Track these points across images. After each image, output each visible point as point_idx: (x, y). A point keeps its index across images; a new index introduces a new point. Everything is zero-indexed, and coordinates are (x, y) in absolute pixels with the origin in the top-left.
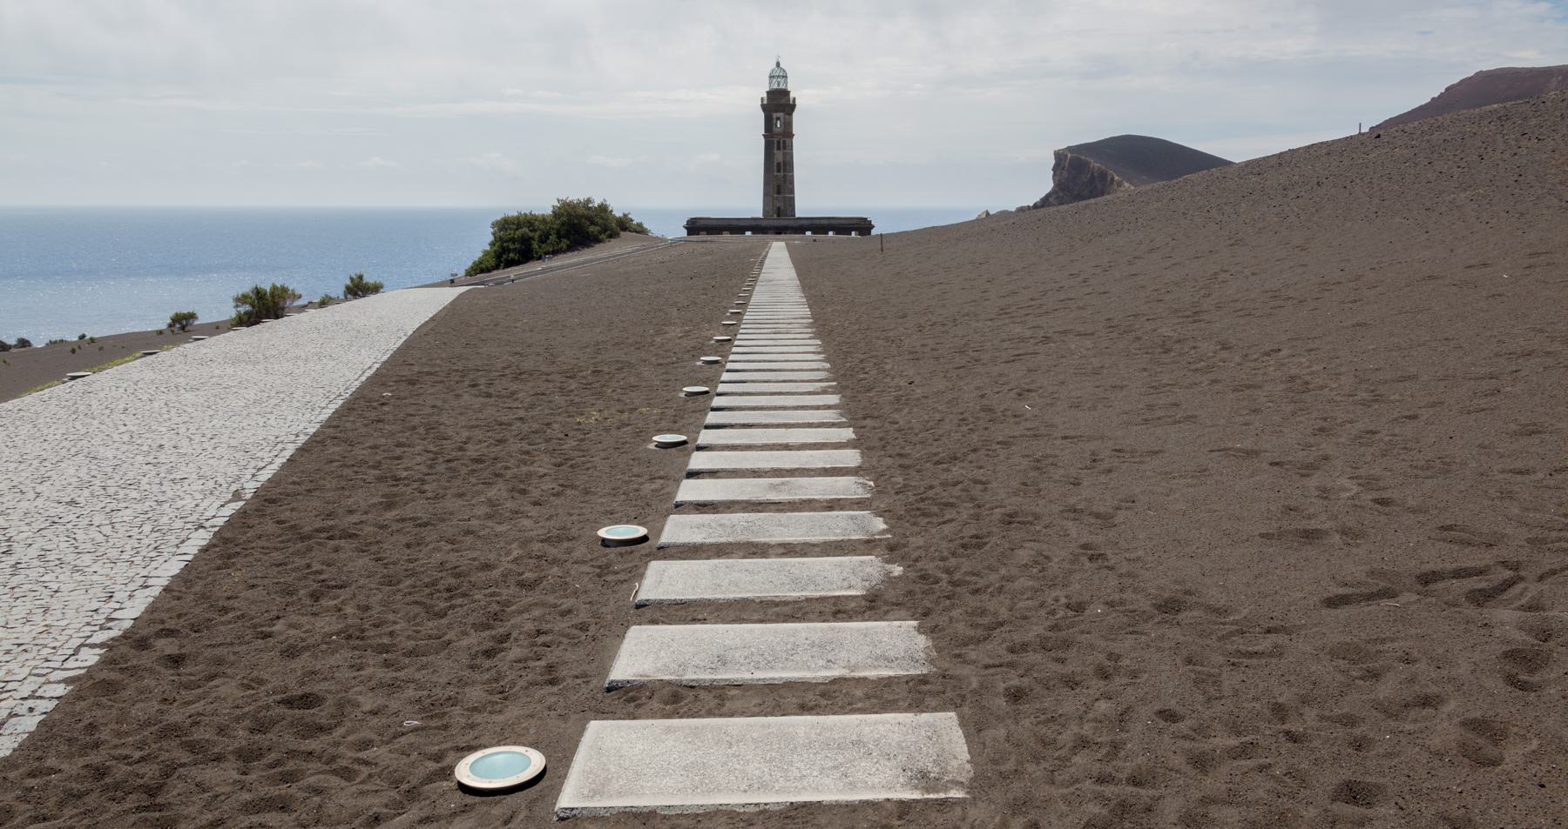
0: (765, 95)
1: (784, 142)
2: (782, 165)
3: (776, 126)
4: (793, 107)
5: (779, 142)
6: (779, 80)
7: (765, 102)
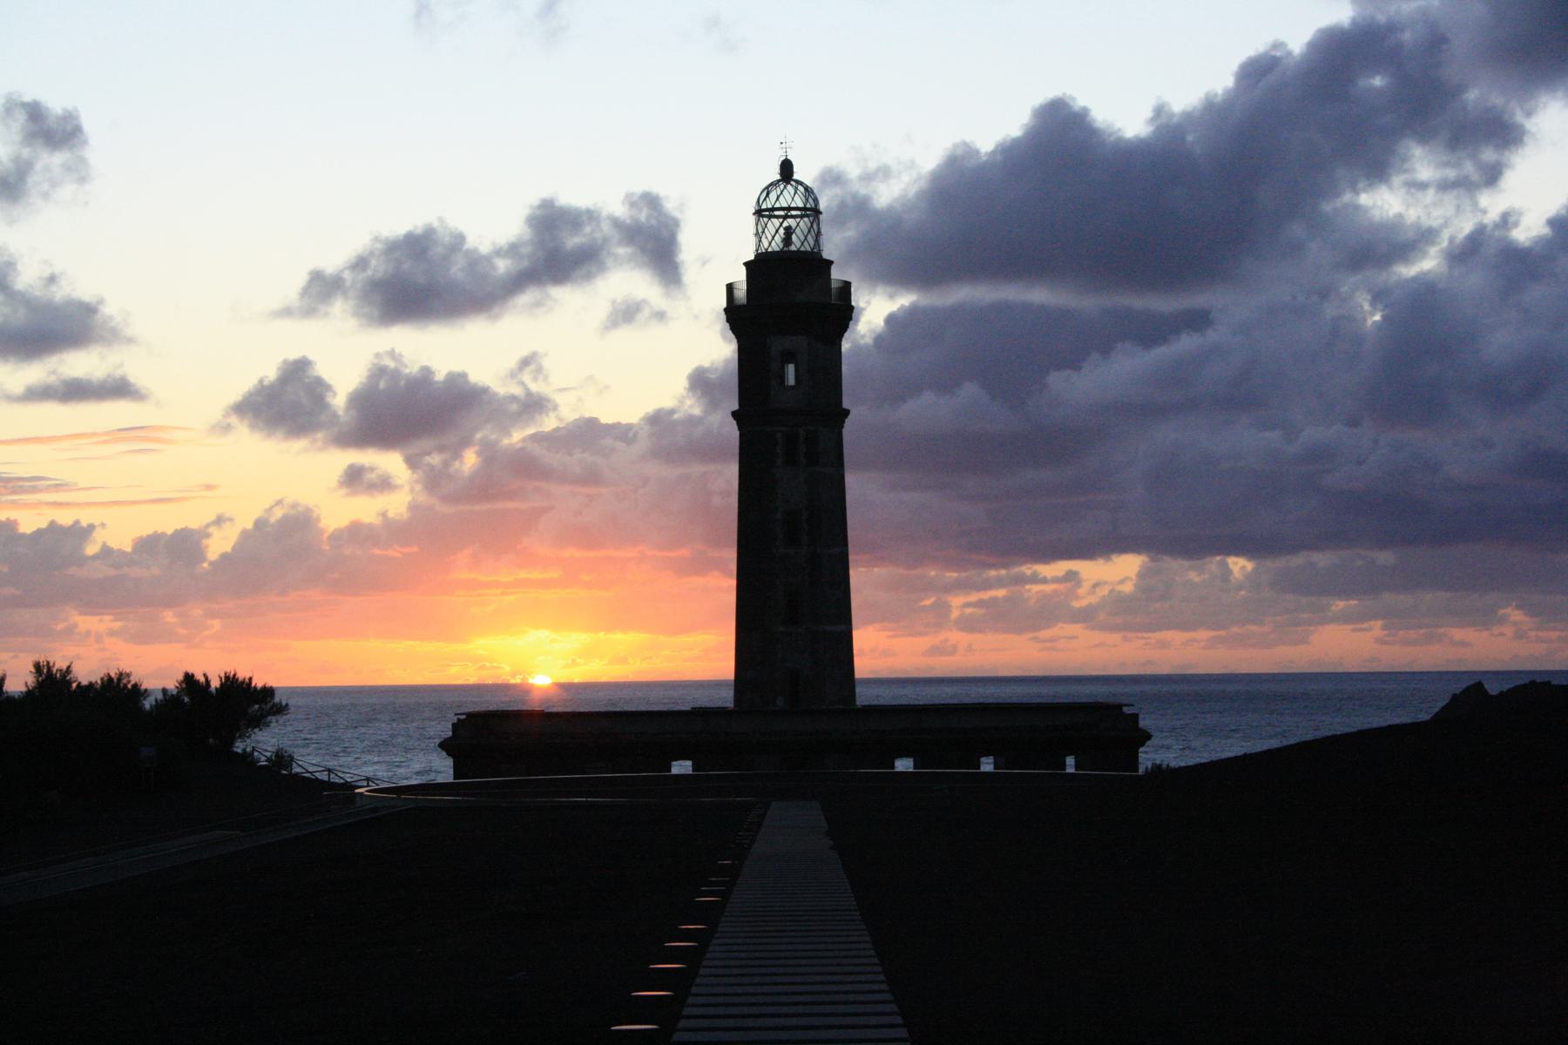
0: (740, 276)
3: (782, 377)
6: (792, 222)
7: (741, 293)
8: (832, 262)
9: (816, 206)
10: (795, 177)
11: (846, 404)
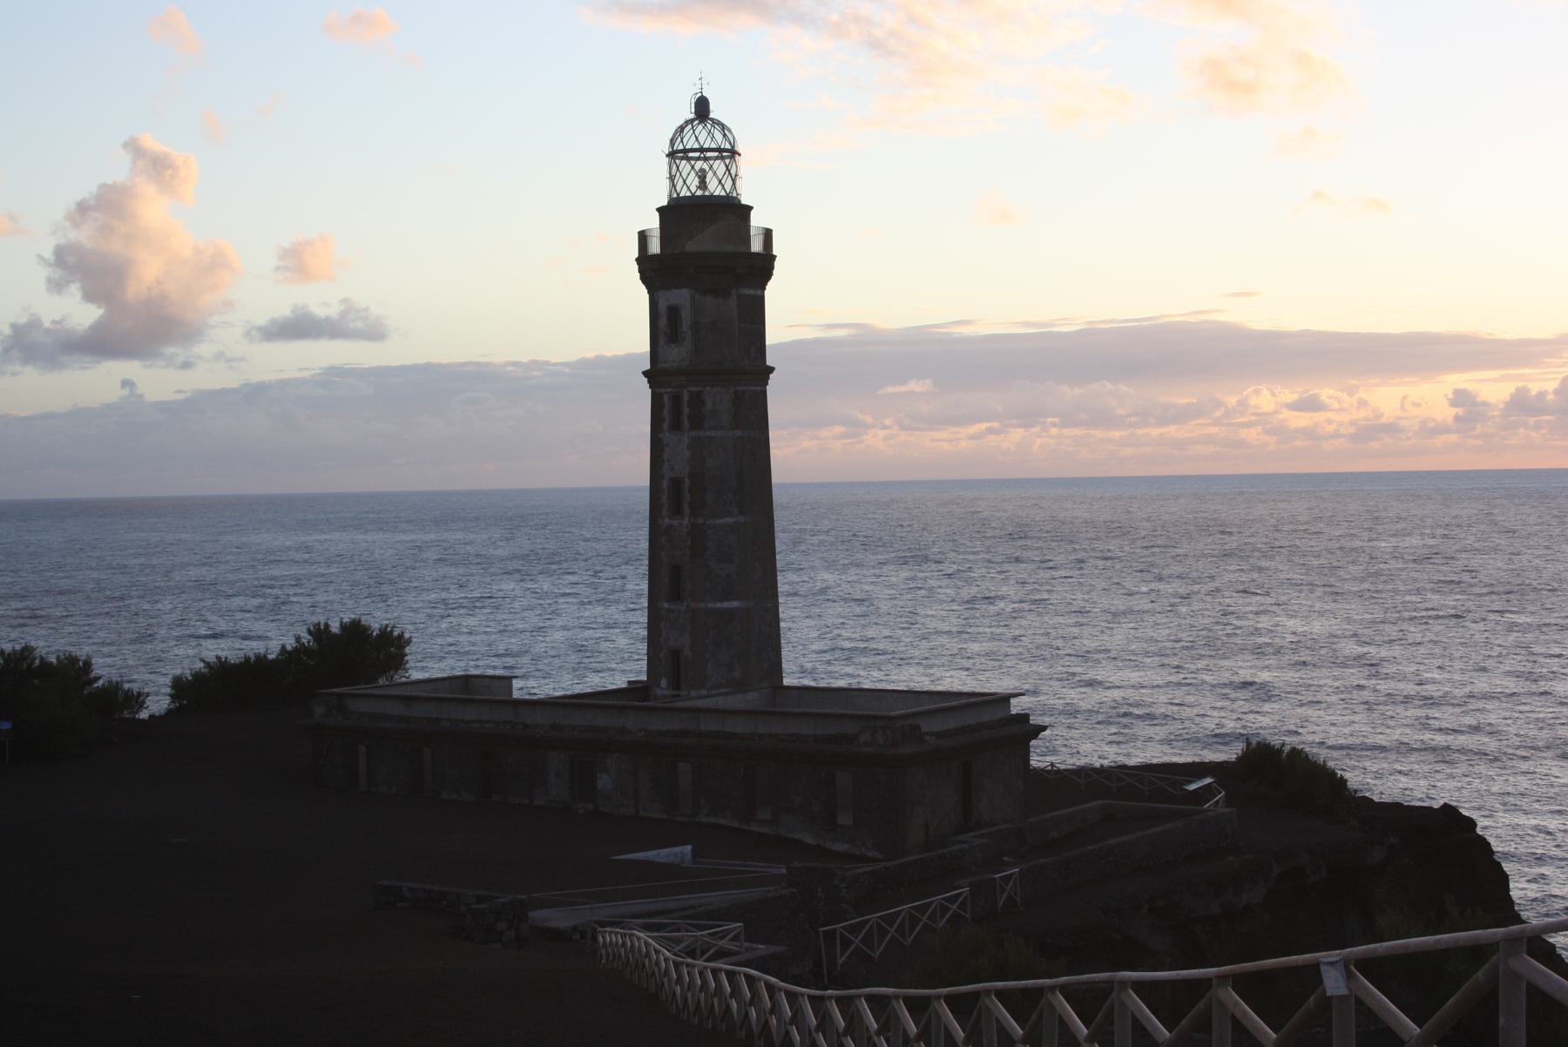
0: (653, 223)
1: (697, 401)
2: (687, 481)
4: (763, 266)
5: (676, 399)
8: (751, 208)
9: (733, 147)
10: (712, 115)
11: (769, 362)
